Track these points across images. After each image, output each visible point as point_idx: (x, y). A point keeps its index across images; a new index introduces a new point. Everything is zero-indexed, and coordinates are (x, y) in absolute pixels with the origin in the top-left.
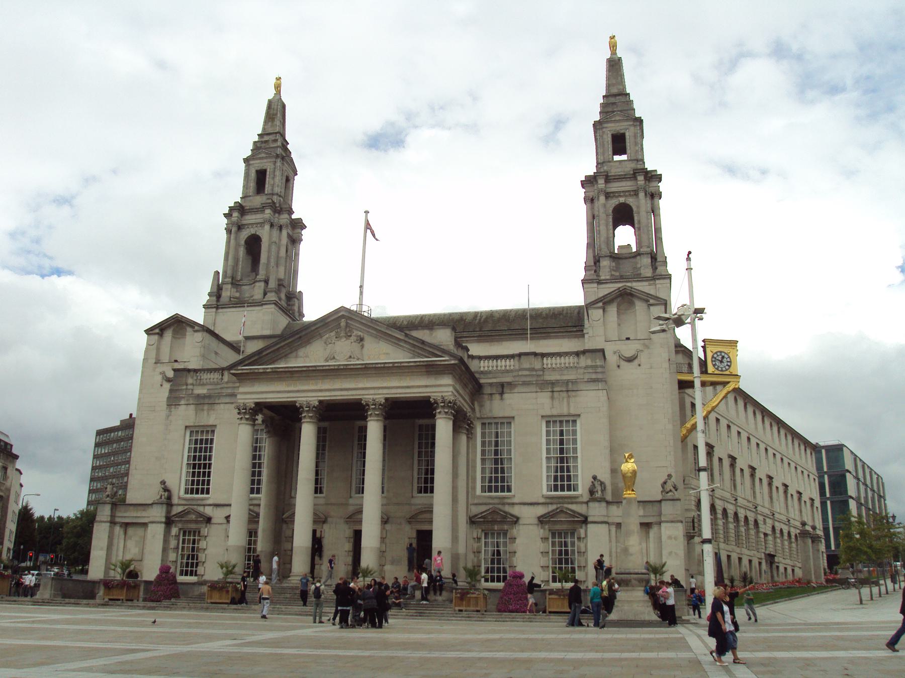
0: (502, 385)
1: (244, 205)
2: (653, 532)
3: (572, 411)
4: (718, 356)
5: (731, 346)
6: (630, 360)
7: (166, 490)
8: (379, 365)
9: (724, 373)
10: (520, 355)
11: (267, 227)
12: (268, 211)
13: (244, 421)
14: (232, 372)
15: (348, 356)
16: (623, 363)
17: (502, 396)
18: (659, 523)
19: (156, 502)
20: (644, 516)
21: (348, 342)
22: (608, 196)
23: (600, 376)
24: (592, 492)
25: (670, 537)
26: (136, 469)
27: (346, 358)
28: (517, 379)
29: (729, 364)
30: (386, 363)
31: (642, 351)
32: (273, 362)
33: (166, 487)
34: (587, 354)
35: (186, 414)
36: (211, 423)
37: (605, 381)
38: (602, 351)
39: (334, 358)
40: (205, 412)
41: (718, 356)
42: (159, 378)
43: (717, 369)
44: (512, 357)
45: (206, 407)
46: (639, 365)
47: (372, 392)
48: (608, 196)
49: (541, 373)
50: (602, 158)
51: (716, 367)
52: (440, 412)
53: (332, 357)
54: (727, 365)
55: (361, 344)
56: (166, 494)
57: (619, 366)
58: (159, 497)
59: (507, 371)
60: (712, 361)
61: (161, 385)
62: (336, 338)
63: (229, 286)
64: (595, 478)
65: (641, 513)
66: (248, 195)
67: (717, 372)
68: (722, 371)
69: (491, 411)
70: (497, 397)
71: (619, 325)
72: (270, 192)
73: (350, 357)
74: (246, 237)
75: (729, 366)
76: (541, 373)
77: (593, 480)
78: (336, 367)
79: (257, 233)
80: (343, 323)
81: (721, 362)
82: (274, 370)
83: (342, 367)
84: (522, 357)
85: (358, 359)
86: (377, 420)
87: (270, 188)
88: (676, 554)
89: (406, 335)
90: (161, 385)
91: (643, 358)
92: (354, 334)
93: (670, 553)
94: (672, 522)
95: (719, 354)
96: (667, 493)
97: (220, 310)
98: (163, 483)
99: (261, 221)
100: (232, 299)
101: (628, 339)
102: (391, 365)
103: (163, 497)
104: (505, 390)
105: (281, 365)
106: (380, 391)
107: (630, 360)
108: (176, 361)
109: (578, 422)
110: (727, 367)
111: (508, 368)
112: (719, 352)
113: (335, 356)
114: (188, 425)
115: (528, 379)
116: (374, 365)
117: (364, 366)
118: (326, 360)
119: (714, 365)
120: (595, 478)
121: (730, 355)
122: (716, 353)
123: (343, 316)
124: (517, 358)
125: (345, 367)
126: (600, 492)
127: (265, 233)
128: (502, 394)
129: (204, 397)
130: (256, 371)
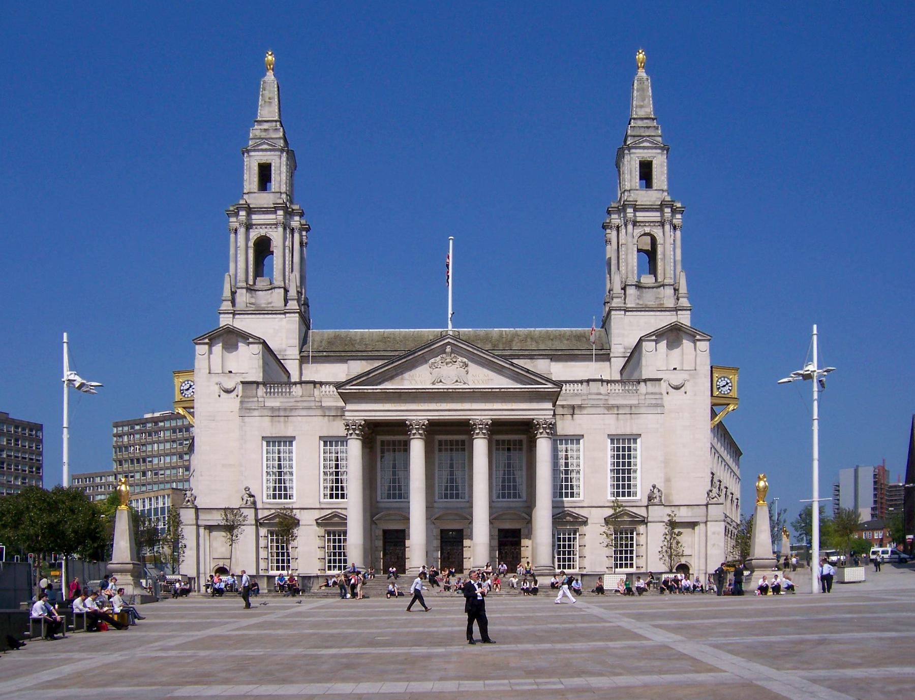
0: (573, 407)
1: (248, 202)
2: (699, 529)
3: (635, 432)
6: (677, 388)
7: (251, 496)
8: (487, 390)
10: (588, 381)
11: (280, 229)
12: (280, 213)
13: (354, 436)
14: (339, 391)
15: (455, 381)
16: (671, 390)
17: (572, 417)
18: (706, 522)
19: (243, 506)
20: (691, 517)
21: (454, 367)
22: (635, 223)
23: (659, 402)
24: (650, 498)
25: (714, 533)
26: (202, 476)
27: (453, 382)
28: (586, 402)
30: (493, 388)
31: (688, 380)
32: (380, 384)
33: (250, 492)
34: (648, 383)
35: (263, 426)
36: (289, 434)
37: (664, 406)
38: (660, 380)
39: (441, 381)
40: (282, 424)
42: (217, 388)
44: (581, 382)
45: (282, 419)
46: (686, 393)
47: (479, 413)
48: (635, 223)
49: (607, 397)
50: (629, 185)
52: (541, 433)
53: (439, 381)
55: (466, 369)
56: (252, 499)
57: (668, 393)
58: (245, 502)
59: (576, 395)
61: (219, 396)
62: (442, 363)
63: (244, 291)
64: (654, 487)
65: (690, 514)
66: (252, 191)
69: (563, 429)
70: (570, 416)
71: (667, 356)
72: (277, 190)
73: (457, 381)
74: (256, 238)
76: (607, 397)
77: (652, 489)
78: (445, 390)
79: (268, 235)
80: (448, 349)
82: (383, 391)
83: (451, 390)
84: (590, 383)
85: (465, 383)
86: (484, 438)
87: (277, 185)
88: (718, 545)
89: (512, 364)
90: (219, 396)
91: (688, 387)
92: (459, 360)
93: (714, 545)
94: (716, 521)
96: (713, 499)
97: (237, 316)
98: (247, 489)
99: (274, 222)
100: (248, 305)
101: (675, 369)
102: (498, 390)
103: (249, 503)
104: (576, 412)
105: (387, 386)
106: (486, 413)
107: (677, 388)
108: (230, 372)
109: (638, 441)
111: (576, 391)
113: (442, 380)
114: (265, 435)
115: (595, 402)
116: (482, 390)
117: (472, 390)
118: (433, 384)
120: (654, 487)
123: (449, 343)
124: (585, 384)
125: (454, 390)
126: (658, 498)
127: (276, 236)
128: (573, 414)
129: (279, 409)
130: (366, 391)
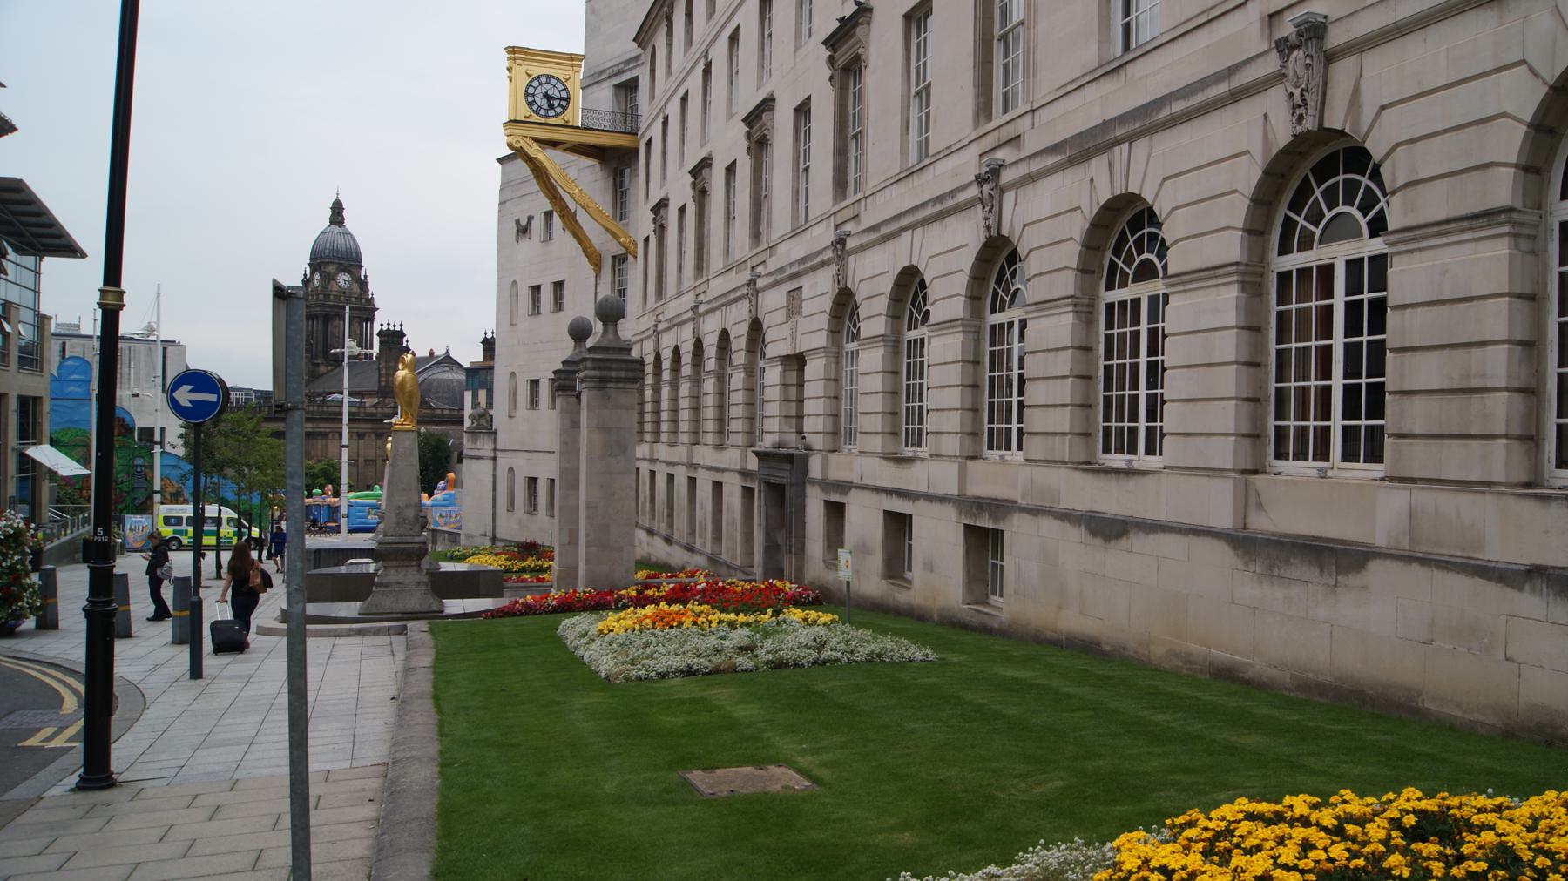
4: (541, 84)
5: (573, 65)
9: (550, 121)
29: (564, 103)
41: (541, 84)
43: (536, 112)
51: (535, 107)
54: (560, 105)
60: (527, 94)
67: (535, 118)
68: (547, 116)
75: (565, 108)
81: (546, 96)
95: (543, 80)
110: (559, 110)
112: (542, 76)
119: (530, 104)
121: (569, 85)
122: (538, 78)
